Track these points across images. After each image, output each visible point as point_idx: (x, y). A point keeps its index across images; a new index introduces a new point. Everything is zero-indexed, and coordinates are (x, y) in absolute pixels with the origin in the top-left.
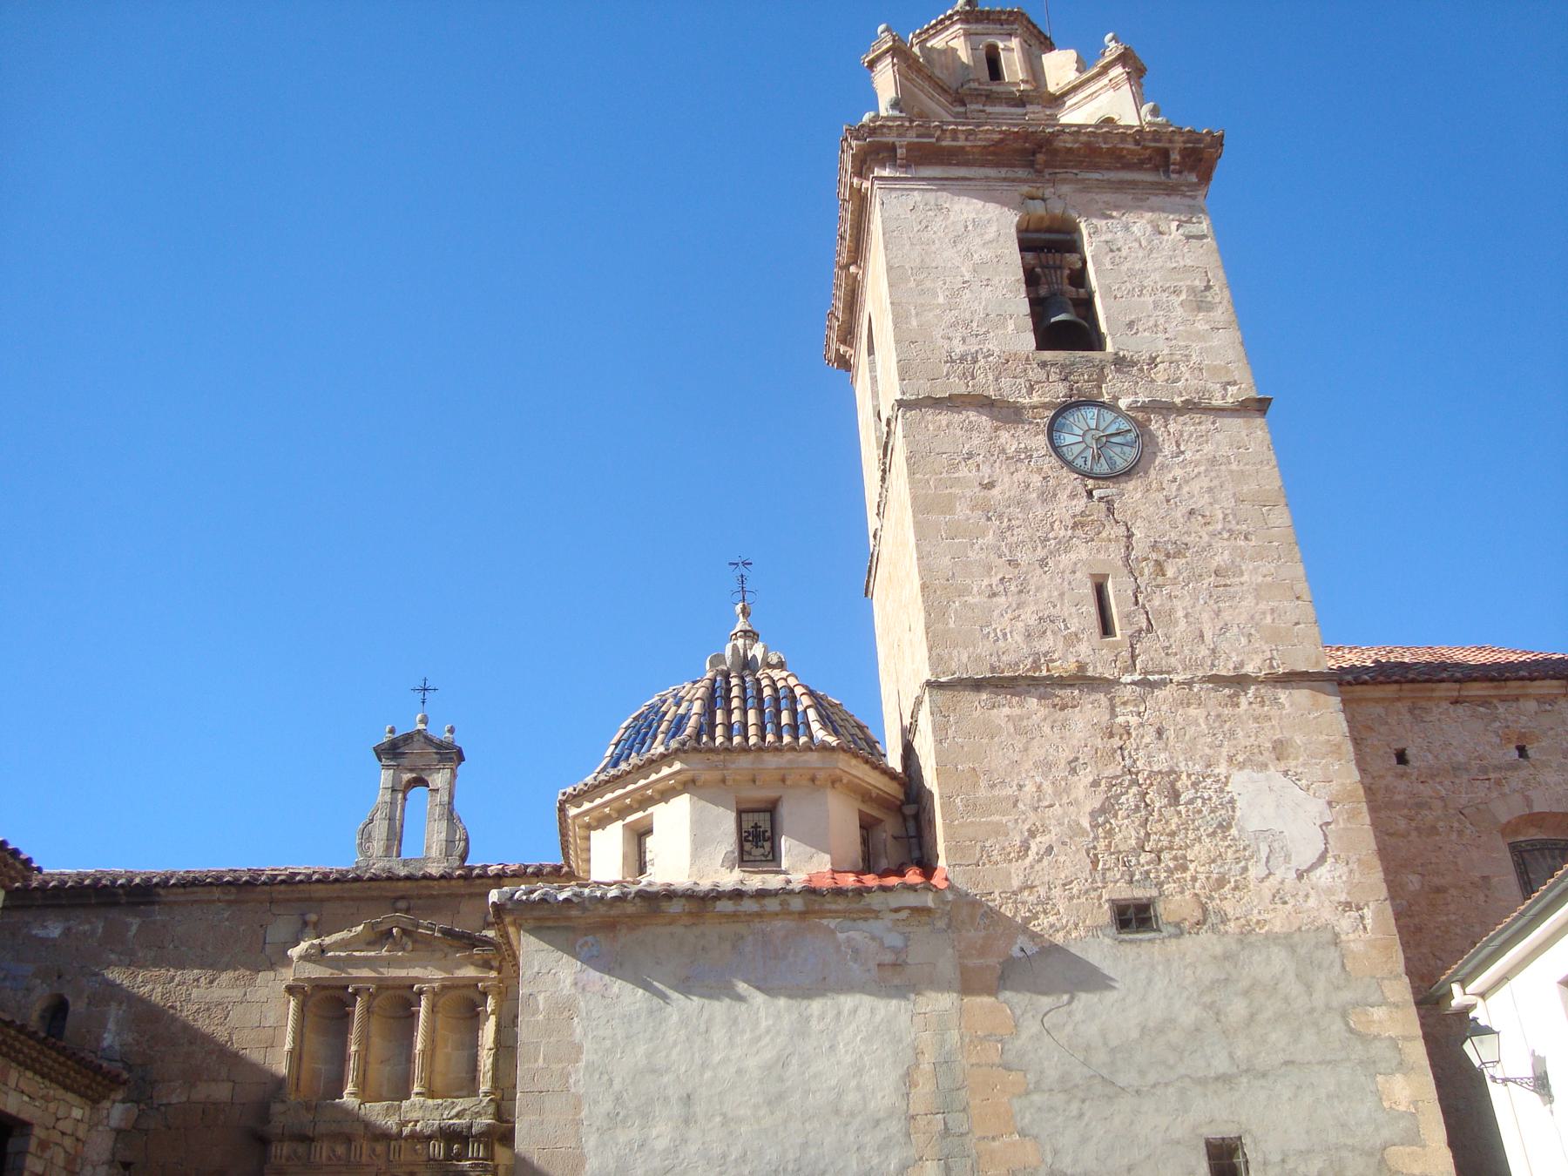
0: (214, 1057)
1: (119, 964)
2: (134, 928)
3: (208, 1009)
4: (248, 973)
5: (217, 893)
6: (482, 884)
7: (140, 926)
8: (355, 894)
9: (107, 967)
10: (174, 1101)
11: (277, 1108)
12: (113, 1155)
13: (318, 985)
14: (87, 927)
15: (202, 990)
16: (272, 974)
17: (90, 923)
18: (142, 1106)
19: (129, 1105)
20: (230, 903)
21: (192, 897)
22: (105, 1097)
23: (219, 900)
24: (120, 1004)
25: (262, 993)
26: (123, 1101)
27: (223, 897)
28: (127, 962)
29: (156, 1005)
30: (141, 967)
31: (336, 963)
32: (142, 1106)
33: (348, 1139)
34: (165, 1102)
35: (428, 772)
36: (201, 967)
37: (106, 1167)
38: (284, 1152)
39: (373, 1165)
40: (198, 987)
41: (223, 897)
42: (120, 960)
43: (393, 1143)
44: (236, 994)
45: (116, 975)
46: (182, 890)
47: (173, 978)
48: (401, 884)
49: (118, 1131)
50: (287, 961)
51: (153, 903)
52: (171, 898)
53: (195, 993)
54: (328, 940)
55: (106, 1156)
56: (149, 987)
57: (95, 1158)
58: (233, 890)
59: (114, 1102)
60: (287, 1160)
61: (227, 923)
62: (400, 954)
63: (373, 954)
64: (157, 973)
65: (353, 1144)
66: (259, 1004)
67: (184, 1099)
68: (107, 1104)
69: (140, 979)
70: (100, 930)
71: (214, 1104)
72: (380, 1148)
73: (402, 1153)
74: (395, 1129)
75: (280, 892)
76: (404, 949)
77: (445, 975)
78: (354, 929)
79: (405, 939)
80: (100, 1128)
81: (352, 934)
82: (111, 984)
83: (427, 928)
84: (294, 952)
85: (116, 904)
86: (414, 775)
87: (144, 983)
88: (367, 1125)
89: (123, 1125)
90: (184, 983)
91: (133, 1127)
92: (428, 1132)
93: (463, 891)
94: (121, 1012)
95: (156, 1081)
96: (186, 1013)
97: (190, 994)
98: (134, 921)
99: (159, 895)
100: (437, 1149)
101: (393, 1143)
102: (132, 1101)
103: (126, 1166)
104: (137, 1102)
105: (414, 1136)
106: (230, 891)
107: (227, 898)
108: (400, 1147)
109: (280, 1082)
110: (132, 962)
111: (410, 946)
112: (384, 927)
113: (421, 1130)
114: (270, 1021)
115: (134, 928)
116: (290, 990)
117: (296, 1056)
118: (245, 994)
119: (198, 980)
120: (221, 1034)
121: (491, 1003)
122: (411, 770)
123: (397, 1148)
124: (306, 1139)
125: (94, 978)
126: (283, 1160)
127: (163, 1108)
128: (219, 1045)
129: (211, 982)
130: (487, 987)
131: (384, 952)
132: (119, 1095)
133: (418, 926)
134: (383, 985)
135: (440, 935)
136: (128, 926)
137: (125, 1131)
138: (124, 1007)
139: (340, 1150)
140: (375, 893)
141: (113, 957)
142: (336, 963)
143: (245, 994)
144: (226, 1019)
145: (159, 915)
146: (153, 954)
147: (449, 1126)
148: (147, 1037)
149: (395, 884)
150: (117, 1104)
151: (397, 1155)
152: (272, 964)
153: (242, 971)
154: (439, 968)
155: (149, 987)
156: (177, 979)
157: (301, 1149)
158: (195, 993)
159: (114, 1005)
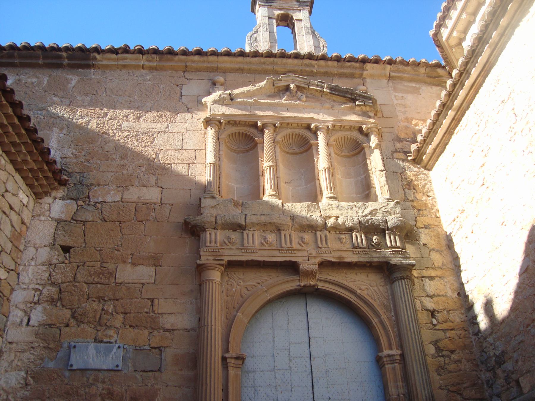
0: (144, 169)
1: (61, 103)
2: (73, 83)
3: (136, 136)
4: (169, 113)
5: (142, 60)
6: (350, 67)
7: (78, 81)
8: (254, 67)
9: (52, 106)
10: (109, 199)
11: (207, 202)
12: (54, 240)
13: (232, 122)
14: (35, 80)
15: (131, 123)
16: (189, 115)
17: (37, 77)
18: (80, 203)
19: (68, 201)
20: (152, 69)
21: (121, 62)
22: (47, 194)
23: (143, 67)
24: (61, 130)
25: (182, 128)
26: (63, 199)
27: (147, 64)
28: (68, 102)
29: (93, 131)
30: (79, 107)
31: (243, 106)
32: (80, 203)
33: (278, 229)
34: (100, 200)
35: (292, 11)
36: (129, 108)
37: (48, 249)
38: (219, 238)
39: (304, 250)
40: (127, 121)
41: (147, 64)
42: (62, 102)
43: (319, 233)
44: (160, 126)
45: (60, 111)
46: (114, 56)
47: (106, 114)
48: (290, 61)
49: (59, 221)
50: (202, 107)
51: (88, 66)
52: (105, 62)
53: (125, 125)
54: (236, 91)
55: (49, 240)
56: (87, 119)
57: (38, 241)
58: (156, 57)
59: (55, 198)
60: (221, 245)
61: (149, 82)
62: (296, 103)
63: (275, 101)
64: (93, 111)
65: (283, 233)
66: (181, 134)
67: (118, 198)
68: (48, 200)
69: (78, 113)
70: (45, 82)
71: (145, 204)
72: (308, 237)
73: (329, 241)
74: (320, 221)
75: (193, 62)
76: (299, 100)
77: (333, 119)
78: (257, 85)
79: (299, 94)
80: (42, 218)
81: (256, 88)
82: (56, 117)
83: (317, 86)
84: (208, 100)
85: (59, 66)
86: (282, 12)
87: (81, 116)
88: (293, 217)
89: (63, 217)
90: (115, 118)
91: (72, 219)
92: (349, 224)
93: (335, 71)
94: (62, 135)
95: (92, 184)
96: (119, 137)
97: (121, 125)
98: (73, 78)
99: (95, 59)
100: (359, 238)
101: (319, 233)
102: (72, 199)
103: (66, 249)
104: (76, 200)
105: (336, 228)
106: (153, 58)
107: (151, 64)
108: (326, 236)
109: (205, 188)
110: (71, 103)
111: (304, 98)
112: (283, 84)
113: (344, 223)
114: (191, 145)
115: (73, 83)
116: (208, 122)
117: (217, 167)
118: (168, 127)
119: (127, 117)
120: (149, 152)
121: (374, 140)
122: (280, 9)
123: (323, 237)
124: (239, 228)
125: (39, 112)
126: (218, 245)
127: (99, 206)
128: (148, 160)
129: (139, 118)
130: (370, 128)
131: (283, 101)
132: (60, 193)
133: (309, 84)
134: (286, 123)
135: (328, 91)
136: (68, 81)
137: (65, 221)
138: (64, 131)
139: (271, 237)
140: (269, 67)
141: (55, 99)
142: (243, 106)
143: (168, 127)
144: (152, 143)
145: (93, 75)
146: (89, 99)
147: (368, 220)
148: (83, 153)
149: (284, 60)
150: (57, 200)
151: (324, 242)
152: (188, 109)
153: (163, 113)
154: (329, 115)
155: (87, 119)
156: (109, 116)
157: (235, 236)
158: (125, 125)
159: (56, 130)
